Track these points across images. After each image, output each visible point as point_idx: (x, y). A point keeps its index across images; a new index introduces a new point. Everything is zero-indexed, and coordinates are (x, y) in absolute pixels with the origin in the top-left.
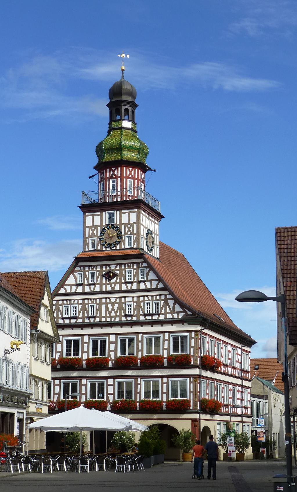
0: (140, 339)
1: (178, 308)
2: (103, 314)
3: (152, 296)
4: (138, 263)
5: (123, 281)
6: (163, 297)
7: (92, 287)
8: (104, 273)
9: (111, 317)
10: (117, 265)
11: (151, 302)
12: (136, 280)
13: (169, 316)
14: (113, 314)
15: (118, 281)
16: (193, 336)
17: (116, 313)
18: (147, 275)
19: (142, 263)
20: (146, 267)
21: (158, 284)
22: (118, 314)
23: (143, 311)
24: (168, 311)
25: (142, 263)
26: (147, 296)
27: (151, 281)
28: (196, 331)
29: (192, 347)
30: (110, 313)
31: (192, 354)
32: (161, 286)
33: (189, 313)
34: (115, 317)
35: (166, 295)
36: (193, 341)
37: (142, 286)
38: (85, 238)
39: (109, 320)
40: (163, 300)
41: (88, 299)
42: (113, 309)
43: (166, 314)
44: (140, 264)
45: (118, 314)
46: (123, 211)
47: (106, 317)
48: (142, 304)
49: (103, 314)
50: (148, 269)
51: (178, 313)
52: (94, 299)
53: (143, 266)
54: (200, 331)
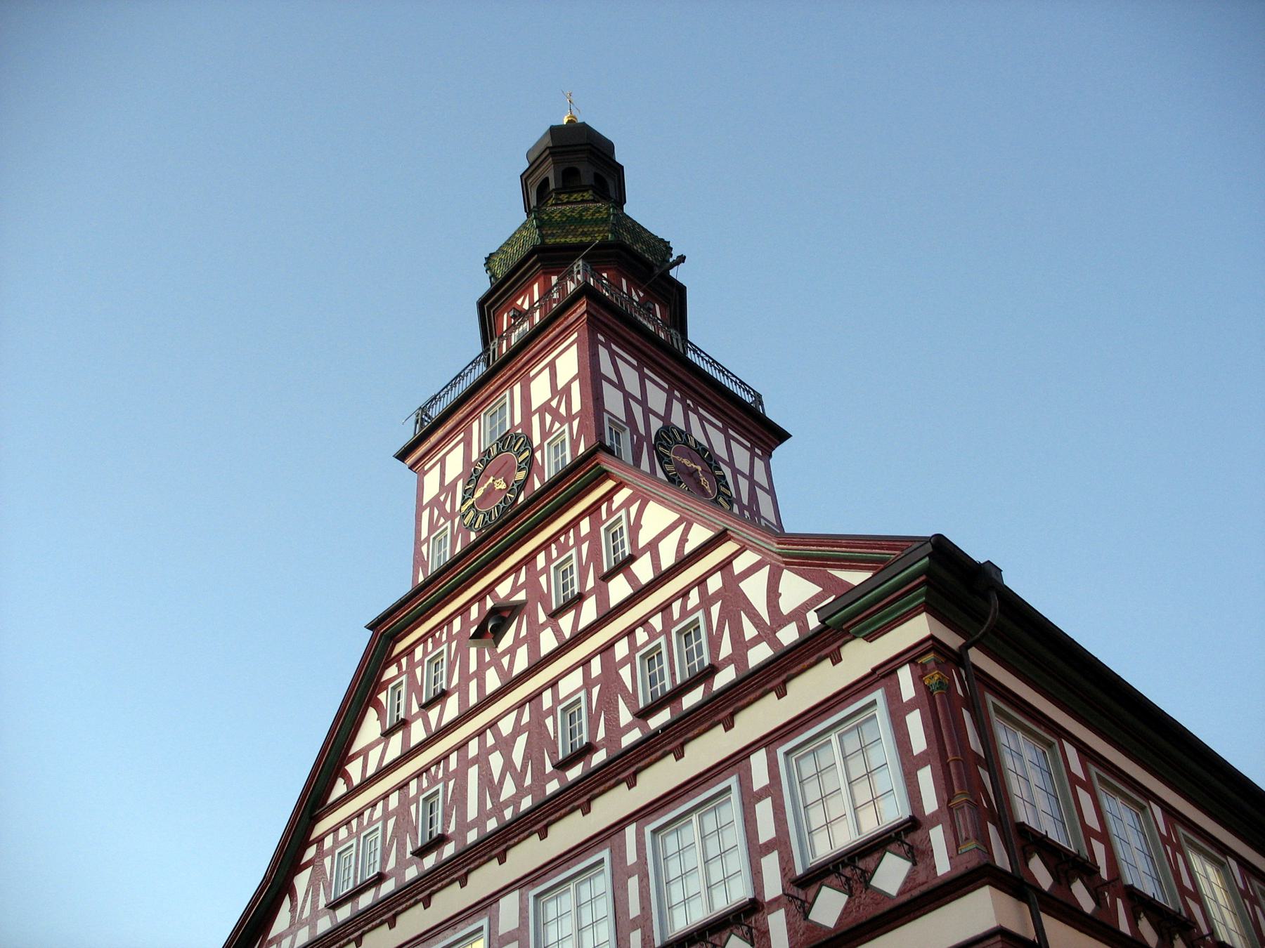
0: (632, 858)
1: (797, 590)
2: (472, 813)
3: (665, 608)
4: (593, 510)
5: (542, 618)
6: (715, 583)
7: (433, 714)
8: (473, 630)
9: (499, 808)
10: (515, 569)
11: (662, 640)
12: (590, 583)
13: (759, 655)
14: (509, 789)
15: (523, 632)
16: (908, 690)
17: (519, 779)
18: (635, 528)
19: (608, 497)
20: (627, 504)
21: (683, 540)
22: (528, 781)
23: (631, 699)
24: (750, 631)
25: (608, 497)
26: (643, 622)
27: (653, 546)
28: (910, 656)
29: (922, 760)
30: (496, 790)
31: (930, 803)
32: (699, 535)
33: (855, 578)
34: (515, 800)
35: (725, 565)
36: (914, 721)
37: (619, 589)
38: (418, 543)
39: (492, 825)
40: (717, 596)
41: (418, 775)
42: (508, 765)
43: (739, 657)
44: (604, 507)
45: (528, 781)
46: (532, 374)
47: (480, 821)
48: (625, 673)
49: (472, 813)
50: (634, 509)
51: (798, 615)
52: (437, 762)
53: (614, 506)
54: (957, 659)
